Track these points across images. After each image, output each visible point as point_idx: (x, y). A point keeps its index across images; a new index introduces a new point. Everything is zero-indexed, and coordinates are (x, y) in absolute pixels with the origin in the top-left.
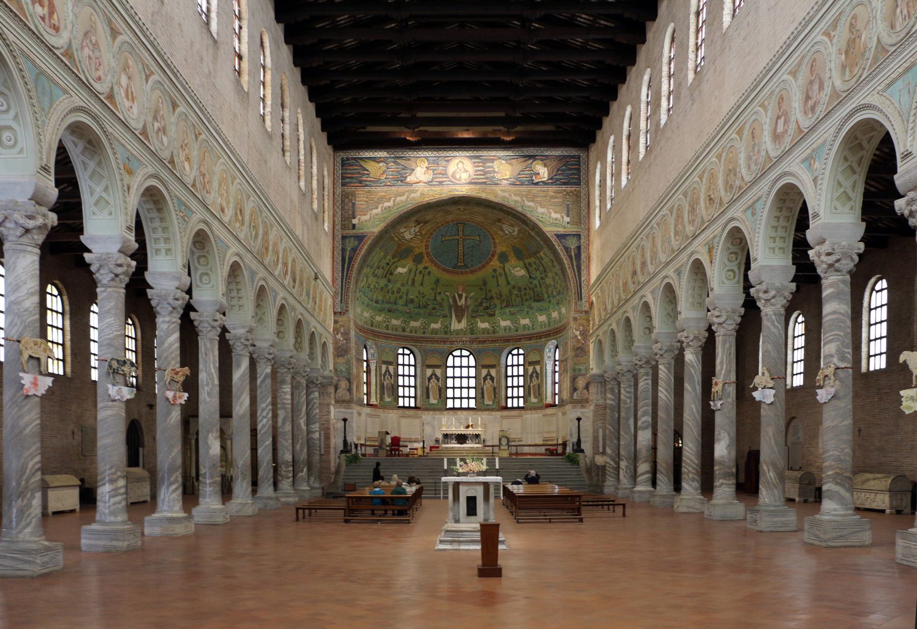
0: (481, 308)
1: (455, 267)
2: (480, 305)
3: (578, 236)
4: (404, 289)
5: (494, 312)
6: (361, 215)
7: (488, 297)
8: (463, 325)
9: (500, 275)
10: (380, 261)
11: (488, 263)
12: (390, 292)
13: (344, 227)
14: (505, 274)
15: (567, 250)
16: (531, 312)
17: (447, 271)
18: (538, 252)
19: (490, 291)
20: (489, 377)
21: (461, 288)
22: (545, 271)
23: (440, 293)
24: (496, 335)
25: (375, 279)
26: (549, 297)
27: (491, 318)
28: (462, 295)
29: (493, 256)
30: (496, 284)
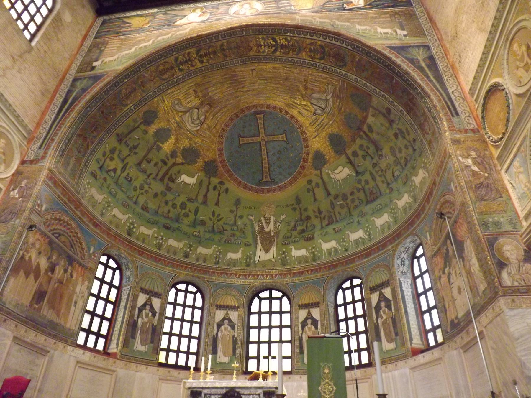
0: (295, 233)
1: (260, 183)
2: (295, 228)
3: (427, 47)
4: (191, 206)
6: (106, 58)
8: (272, 255)
9: (318, 185)
10: (149, 150)
11: (300, 173)
13: (80, 70)
14: (324, 183)
15: (413, 61)
16: (363, 220)
17: (250, 189)
18: (365, 118)
19: (306, 210)
20: (309, 321)
22: (378, 148)
23: (241, 217)
24: (317, 262)
25: (142, 177)
26: (388, 184)
29: (306, 161)
30: (313, 199)
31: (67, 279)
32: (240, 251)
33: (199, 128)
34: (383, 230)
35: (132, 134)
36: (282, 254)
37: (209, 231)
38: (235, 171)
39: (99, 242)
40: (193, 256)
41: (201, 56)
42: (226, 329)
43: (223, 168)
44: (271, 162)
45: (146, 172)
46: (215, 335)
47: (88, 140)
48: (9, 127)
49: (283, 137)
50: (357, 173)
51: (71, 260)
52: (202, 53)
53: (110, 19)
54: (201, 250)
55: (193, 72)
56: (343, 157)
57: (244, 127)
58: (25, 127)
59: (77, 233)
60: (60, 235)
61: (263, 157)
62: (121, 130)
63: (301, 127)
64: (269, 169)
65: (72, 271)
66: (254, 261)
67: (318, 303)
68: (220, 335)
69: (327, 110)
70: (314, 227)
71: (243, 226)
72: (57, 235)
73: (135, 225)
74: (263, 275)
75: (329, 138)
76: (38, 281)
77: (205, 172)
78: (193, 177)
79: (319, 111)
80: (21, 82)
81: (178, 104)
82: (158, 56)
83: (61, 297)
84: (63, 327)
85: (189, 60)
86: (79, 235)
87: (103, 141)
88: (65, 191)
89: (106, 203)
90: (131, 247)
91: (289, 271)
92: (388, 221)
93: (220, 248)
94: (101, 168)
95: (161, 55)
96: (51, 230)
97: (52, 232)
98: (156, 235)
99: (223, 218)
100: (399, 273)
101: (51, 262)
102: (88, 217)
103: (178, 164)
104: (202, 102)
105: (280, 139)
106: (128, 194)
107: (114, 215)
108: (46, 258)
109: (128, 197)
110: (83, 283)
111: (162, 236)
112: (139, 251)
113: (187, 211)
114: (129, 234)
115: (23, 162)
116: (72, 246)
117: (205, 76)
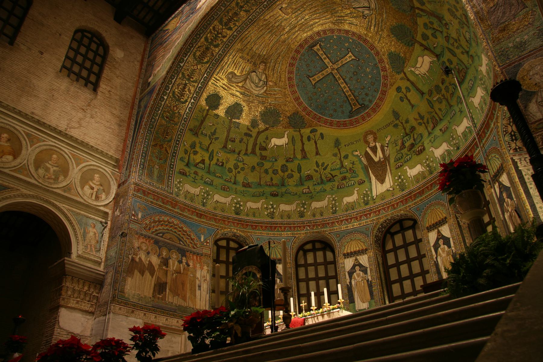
0: (405, 151)
1: (351, 114)
2: (403, 146)
5: (423, 145)
7: (408, 131)
10: (229, 131)
11: (385, 85)
12: (270, 171)
14: (412, 83)
19: (407, 121)
20: (441, 242)
21: (370, 138)
23: (346, 157)
27: (422, 156)
28: (376, 146)
30: (410, 107)
31: (184, 269)
32: (356, 192)
33: (265, 88)
34: (482, 108)
35: (204, 123)
36: (398, 179)
37: (318, 184)
38: (322, 114)
39: (208, 229)
40: (309, 214)
41: (226, 24)
42: (358, 275)
43: (309, 115)
44: (352, 88)
45: (234, 151)
46: (348, 284)
47: (165, 146)
48: (99, 163)
49: (350, 57)
50: (437, 56)
51: (183, 252)
52: (225, 20)
53: (155, 35)
54: (316, 205)
55: (229, 42)
56: (417, 46)
57: (308, 66)
58: (111, 158)
59: (182, 228)
60: (164, 234)
61: (342, 86)
62: (192, 124)
63: (360, 37)
64: (354, 96)
65: (187, 261)
66: (372, 197)
67: (446, 218)
68: (353, 283)
69: (373, 6)
70: (422, 136)
71: (351, 166)
72: (161, 235)
73: (242, 203)
74: (384, 209)
75: (393, 34)
76: (154, 277)
77: (293, 127)
78: (284, 137)
79: (367, 12)
80: (97, 125)
81: (233, 77)
82: (189, 46)
83: (183, 284)
84: (193, 308)
85: (218, 33)
86: (185, 229)
87: (179, 141)
88: (156, 196)
89: (204, 193)
90: (243, 224)
91: (409, 194)
92: (483, 95)
93: (334, 196)
94: (187, 165)
95: (191, 43)
96: (154, 232)
97: (154, 234)
98: (265, 206)
99: (328, 165)
100: (511, 152)
101: (162, 258)
102: (189, 210)
103: (263, 131)
104: (254, 64)
105: (348, 60)
106: (225, 178)
107: (217, 201)
108: (156, 256)
109: (225, 180)
110: (202, 269)
111: (271, 205)
112: (252, 226)
113: (289, 172)
114: (237, 214)
115: (119, 186)
116: (180, 240)
117: (242, 39)
